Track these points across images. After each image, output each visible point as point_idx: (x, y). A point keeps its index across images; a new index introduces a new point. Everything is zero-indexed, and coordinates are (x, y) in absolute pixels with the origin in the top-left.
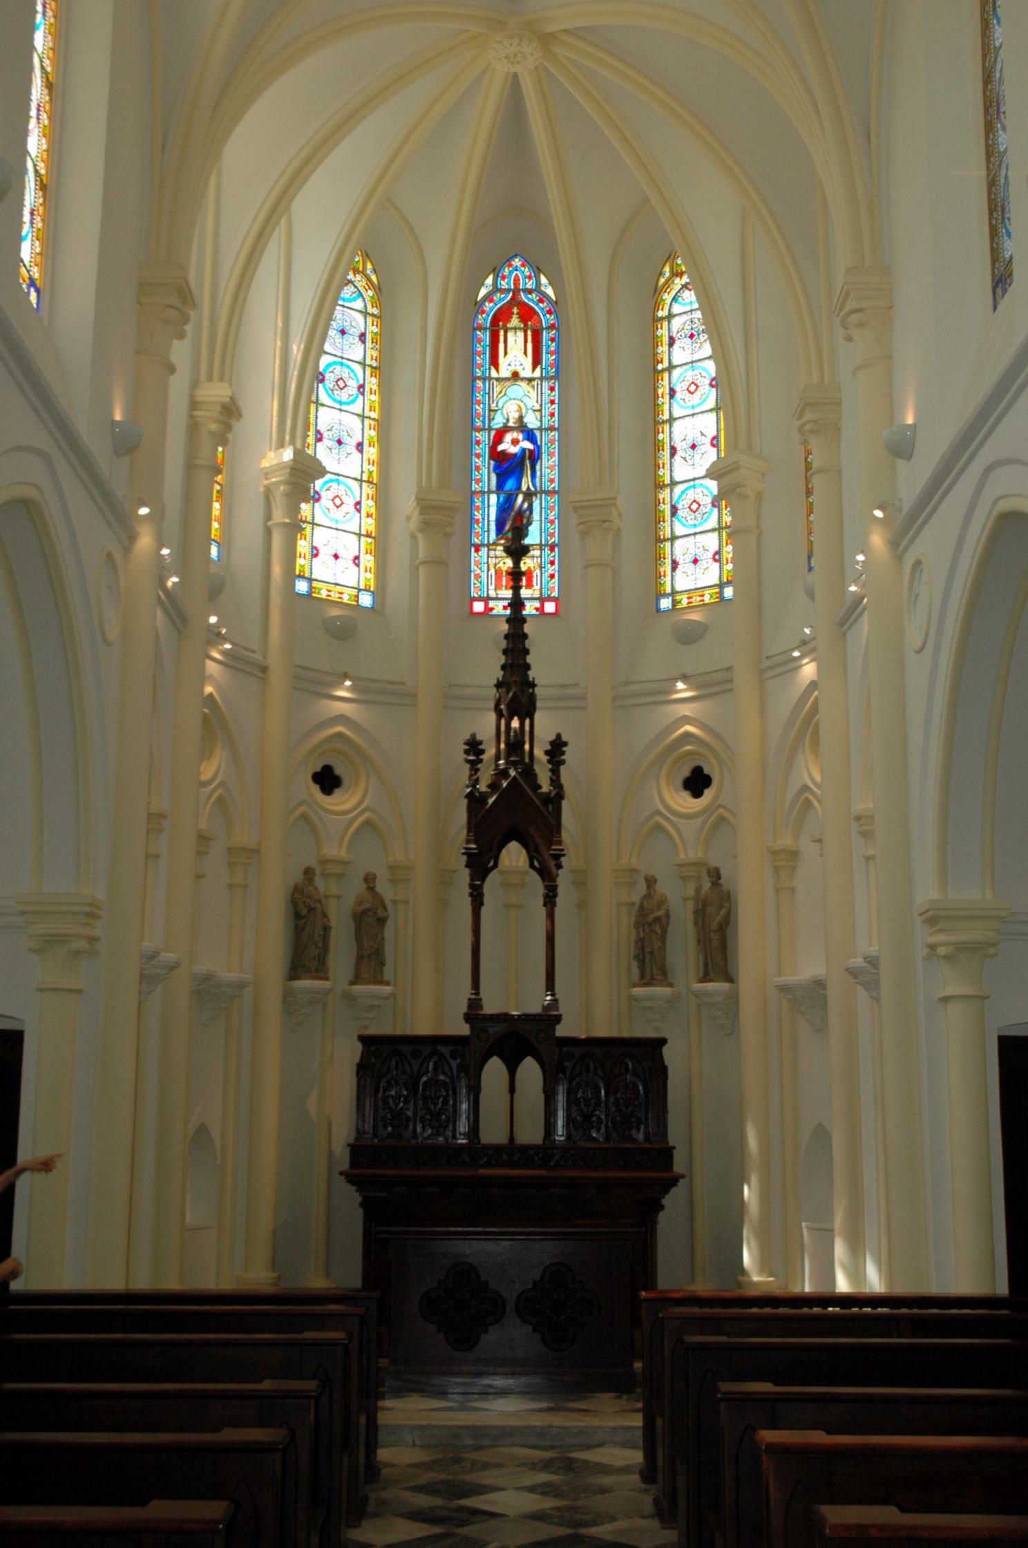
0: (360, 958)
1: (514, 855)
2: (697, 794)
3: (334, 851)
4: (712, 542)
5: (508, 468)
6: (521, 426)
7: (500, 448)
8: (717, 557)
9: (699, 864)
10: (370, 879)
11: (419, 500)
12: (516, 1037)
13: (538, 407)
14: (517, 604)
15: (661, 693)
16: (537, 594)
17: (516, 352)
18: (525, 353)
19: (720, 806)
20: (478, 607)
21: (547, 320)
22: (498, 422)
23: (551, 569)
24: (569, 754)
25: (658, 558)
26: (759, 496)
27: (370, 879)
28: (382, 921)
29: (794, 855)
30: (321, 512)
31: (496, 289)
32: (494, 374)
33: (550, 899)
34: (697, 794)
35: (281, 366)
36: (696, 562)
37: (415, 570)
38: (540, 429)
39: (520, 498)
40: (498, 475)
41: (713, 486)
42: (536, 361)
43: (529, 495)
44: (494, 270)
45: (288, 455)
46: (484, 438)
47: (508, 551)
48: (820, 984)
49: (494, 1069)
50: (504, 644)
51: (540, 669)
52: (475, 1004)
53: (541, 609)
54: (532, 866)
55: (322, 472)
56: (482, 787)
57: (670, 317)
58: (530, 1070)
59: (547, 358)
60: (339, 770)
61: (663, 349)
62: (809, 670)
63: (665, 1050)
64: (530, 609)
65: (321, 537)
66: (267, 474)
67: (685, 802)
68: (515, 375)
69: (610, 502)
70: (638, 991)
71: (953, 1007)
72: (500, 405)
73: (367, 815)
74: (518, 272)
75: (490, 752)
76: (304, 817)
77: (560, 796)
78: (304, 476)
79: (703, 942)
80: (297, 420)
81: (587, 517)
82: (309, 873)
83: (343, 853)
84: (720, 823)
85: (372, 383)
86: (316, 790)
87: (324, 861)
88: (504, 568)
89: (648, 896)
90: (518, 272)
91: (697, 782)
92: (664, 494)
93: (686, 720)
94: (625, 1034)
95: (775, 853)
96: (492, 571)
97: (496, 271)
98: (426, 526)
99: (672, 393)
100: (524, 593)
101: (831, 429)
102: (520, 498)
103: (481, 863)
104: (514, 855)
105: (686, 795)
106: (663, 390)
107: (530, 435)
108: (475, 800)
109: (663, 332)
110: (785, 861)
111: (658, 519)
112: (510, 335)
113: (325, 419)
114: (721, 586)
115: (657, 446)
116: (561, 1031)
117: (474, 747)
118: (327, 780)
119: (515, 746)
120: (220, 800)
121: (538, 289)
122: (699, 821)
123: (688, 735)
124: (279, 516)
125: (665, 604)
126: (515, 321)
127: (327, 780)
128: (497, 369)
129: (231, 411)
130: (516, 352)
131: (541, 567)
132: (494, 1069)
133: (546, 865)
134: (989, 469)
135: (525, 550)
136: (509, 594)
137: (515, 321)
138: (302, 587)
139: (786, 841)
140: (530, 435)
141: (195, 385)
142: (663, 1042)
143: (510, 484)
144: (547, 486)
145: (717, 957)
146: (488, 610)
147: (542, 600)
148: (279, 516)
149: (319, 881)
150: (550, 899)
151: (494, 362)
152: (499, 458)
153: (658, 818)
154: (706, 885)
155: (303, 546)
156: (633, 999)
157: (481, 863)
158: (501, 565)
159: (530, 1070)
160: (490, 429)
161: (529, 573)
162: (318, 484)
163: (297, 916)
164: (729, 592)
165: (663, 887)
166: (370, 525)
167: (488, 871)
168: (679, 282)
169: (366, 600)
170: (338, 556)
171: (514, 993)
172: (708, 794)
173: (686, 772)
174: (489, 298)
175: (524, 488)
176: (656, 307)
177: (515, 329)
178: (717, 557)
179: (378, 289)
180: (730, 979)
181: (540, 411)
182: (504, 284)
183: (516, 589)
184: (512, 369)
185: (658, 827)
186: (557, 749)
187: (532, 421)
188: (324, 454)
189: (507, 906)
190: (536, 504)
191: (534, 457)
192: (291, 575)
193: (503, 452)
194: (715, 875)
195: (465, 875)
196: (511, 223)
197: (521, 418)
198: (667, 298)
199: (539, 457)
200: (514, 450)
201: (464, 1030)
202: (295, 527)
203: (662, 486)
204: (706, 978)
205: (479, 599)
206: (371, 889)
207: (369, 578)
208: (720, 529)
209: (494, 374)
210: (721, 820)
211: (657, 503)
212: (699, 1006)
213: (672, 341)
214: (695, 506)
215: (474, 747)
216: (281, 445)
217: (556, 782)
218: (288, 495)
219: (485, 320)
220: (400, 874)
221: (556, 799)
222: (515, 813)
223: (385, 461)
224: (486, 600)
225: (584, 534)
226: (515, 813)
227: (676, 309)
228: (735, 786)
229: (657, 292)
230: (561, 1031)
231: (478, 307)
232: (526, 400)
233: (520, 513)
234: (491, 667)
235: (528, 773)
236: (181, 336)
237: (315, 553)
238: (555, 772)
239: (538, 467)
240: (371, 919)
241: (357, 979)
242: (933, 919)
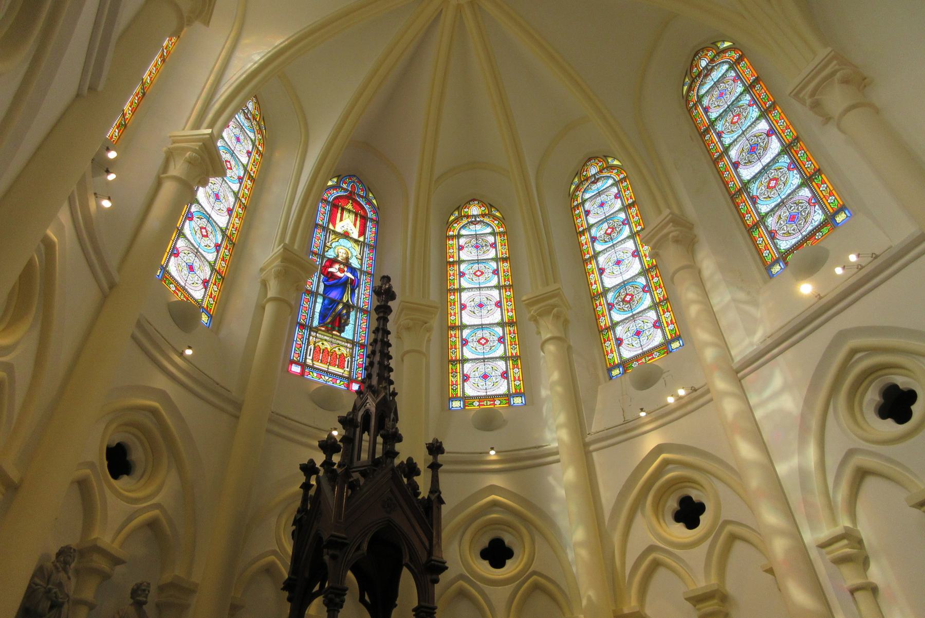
7: (330, 270)
13: (359, 257)
16: (346, 374)
18: (355, 225)
19: (535, 573)
20: (296, 369)
21: (370, 215)
23: (452, 278)
32: (331, 227)
35: (212, 85)
38: (360, 270)
39: (340, 307)
40: (325, 285)
44: (338, 176)
54: (362, 600)
60: (137, 455)
72: (333, 245)
73: (156, 512)
83: (116, 545)
88: (322, 347)
96: (312, 346)
102: (340, 307)
112: (346, 214)
122: (510, 588)
123: (495, 504)
128: (334, 225)
131: (352, 357)
143: (334, 294)
144: (361, 305)
151: (332, 220)
153: (461, 582)
158: (320, 344)
160: (323, 257)
173: (485, 542)
175: (345, 300)
177: (349, 211)
181: (362, 260)
184: (345, 229)
190: (352, 314)
193: (332, 273)
197: (347, 259)
199: (358, 286)
205: (297, 363)
209: (331, 227)
214: (483, 341)
224: (304, 365)
227: (463, 232)
232: (353, 251)
233: (339, 315)
239: (356, 291)
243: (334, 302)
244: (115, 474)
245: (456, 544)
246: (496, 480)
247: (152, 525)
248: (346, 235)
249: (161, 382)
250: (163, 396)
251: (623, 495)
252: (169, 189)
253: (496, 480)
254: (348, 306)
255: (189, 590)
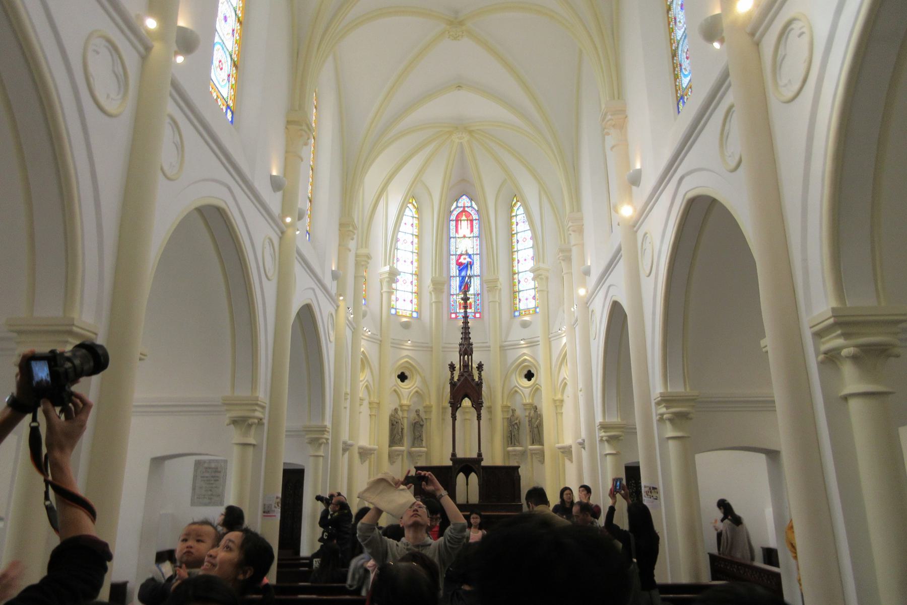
0: (415, 439)
1: (467, 402)
2: (529, 380)
3: (405, 402)
4: (532, 293)
5: (462, 267)
6: (467, 254)
8: (534, 298)
9: (531, 404)
10: (417, 411)
11: (432, 281)
12: (467, 466)
14: (466, 317)
15: (516, 346)
17: (464, 228)
20: (453, 316)
21: (475, 217)
22: (459, 253)
24: (484, 367)
25: (515, 298)
26: (547, 278)
27: (417, 411)
28: (422, 426)
29: (562, 401)
30: (399, 286)
31: (457, 207)
33: (479, 417)
34: (529, 380)
36: (527, 299)
37: (431, 304)
41: (532, 275)
42: (472, 231)
43: (470, 277)
45: (387, 268)
46: (453, 260)
47: (462, 299)
48: (571, 447)
49: (461, 477)
50: (462, 331)
51: (474, 338)
52: (454, 455)
53: (475, 316)
55: (399, 273)
56: (456, 379)
57: (516, 215)
58: (473, 477)
59: (476, 230)
60: (407, 374)
61: (514, 226)
62: (564, 340)
63: (520, 470)
64: (471, 316)
65: (399, 294)
66: (381, 274)
67: (525, 382)
68: (464, 237)
69: (497, 280)
70: (510, 449)
71: (608, 457)
74: (464, 201)
75: (457, 367)
76: (395, 391)
77: (481, 383)
78: (393, 275)
79: (532, 431)
80: (390, 257)
81: (490, 285)
82: (396, 410)
84: (536, 390)
85: (416, 240)
86: (399, 380)
87: (401, 406)
89: (513, 415)
90: (464, 201)
91: (529, 376)
92: (516, 276)
93: (524, 354)
94: (507, 464)
95: (555, 401)
97: (457, 200)
98: (435, 289)
99: (518, 241)
100: (468, 310)
101: (568, 259)
103: (455, 405)
104: (467, 402)
105: (525, 380)
106: (515, 240)
107: (470, 256)
108: (453, 384)
109: (514, 220)
110: (558, 404)
111: (514, 285)
113: (400, 254)
114: (536, 308)
115: (513, 260)
116: (483, 464)
117: (452, 367)
118: (403, 377)
119: (466, 366)
120: (367, 387)
121: (471, 206)
123: (525, 360)
124: (385, 289)
125: (517, 314)
126: (464, 218)
127: (403, 377)
129: (368, 257)
130: (464, 228)
132: (461, 477)
133: (478, 405)
134: (609, 287)
135: (468, 299)
136: (462, 311)
137: (464, 218)
138: (393, 311)
139: (559, 397)
140: (470, 256)
141: (357, 249)
142: (518, 467)
143: (463, 274)
145: (537, 436)
146: (457, 317)
147: (475, 313)
148: (385, 289)
149: (400, 413)
150: (479, 417)
151: (457, 231)
152: (459, 264)
154: (532, 412)
155: (393, 297)
156: (508, 452)
157: (455, 405)
159: (473, 477)
161: (471, 304)
162: (398, 277)
163: (393, 425)
164: (538, 310)
165: (519, 412)
166: (415, 289)
167: (457, 408)
168: (519, 204)
169: (415, 315)
170: (404, 301)
171: (467, 451)
172: (533, 379)
173: (525, 372)
174: (455, 209)
176: (512, 212)
178: (534, 298)
179: (417, 209)
180: (542, 445)
182: (459, 205)
183: (466, 312)
185: (516, 391)
186: (480, 367)
187: (470, 252)
188: (400, 266)
189: (466, 419)
191: (471, 264)
192: (390, 307)
194: (536, 408)
195: (450, 410)
196: (462, 185)
198: (515, 209)
200: (465, 262)
201: (450, 463)
202: (390, 293)
203: (515, 274)
204: (533, 443)
206: (418, 415)
207: (415, 307)
208: (535, 288)
210: (537, 389)
211: (513, 279)
212: (532, 454)
213: (517, 224)
215: (452, 367)
216: (385, 265)
217: (480, 378)
218: (388, 282)
219: (453, 217)
220: (428, 409)
221: (479, 385)
222: (466, 388)
223: (420, 267)
225: (489, 291)
226: (466, 388)
228: (541, 377)
229: (512, 207)
230: (483, 464)
231: (451, 212)
234: (458, 338)
235: (471, 375)
236: (352, 239)
237: (397, 300)
238: (480, 374)
240: (418, 427)
241: (413, 446)
242: (604, 427)
243: (463, 278)
244: (403, 381)
245: (514, 376)
246: (525, 351)
247: (417, 392)
248: (464, 237)
249: (405, 353)
250: (407, 356)
251: (558, 359)
252: (385, 296)
253: (525, 351)
254: (470, 277)
255: (431, 407)
